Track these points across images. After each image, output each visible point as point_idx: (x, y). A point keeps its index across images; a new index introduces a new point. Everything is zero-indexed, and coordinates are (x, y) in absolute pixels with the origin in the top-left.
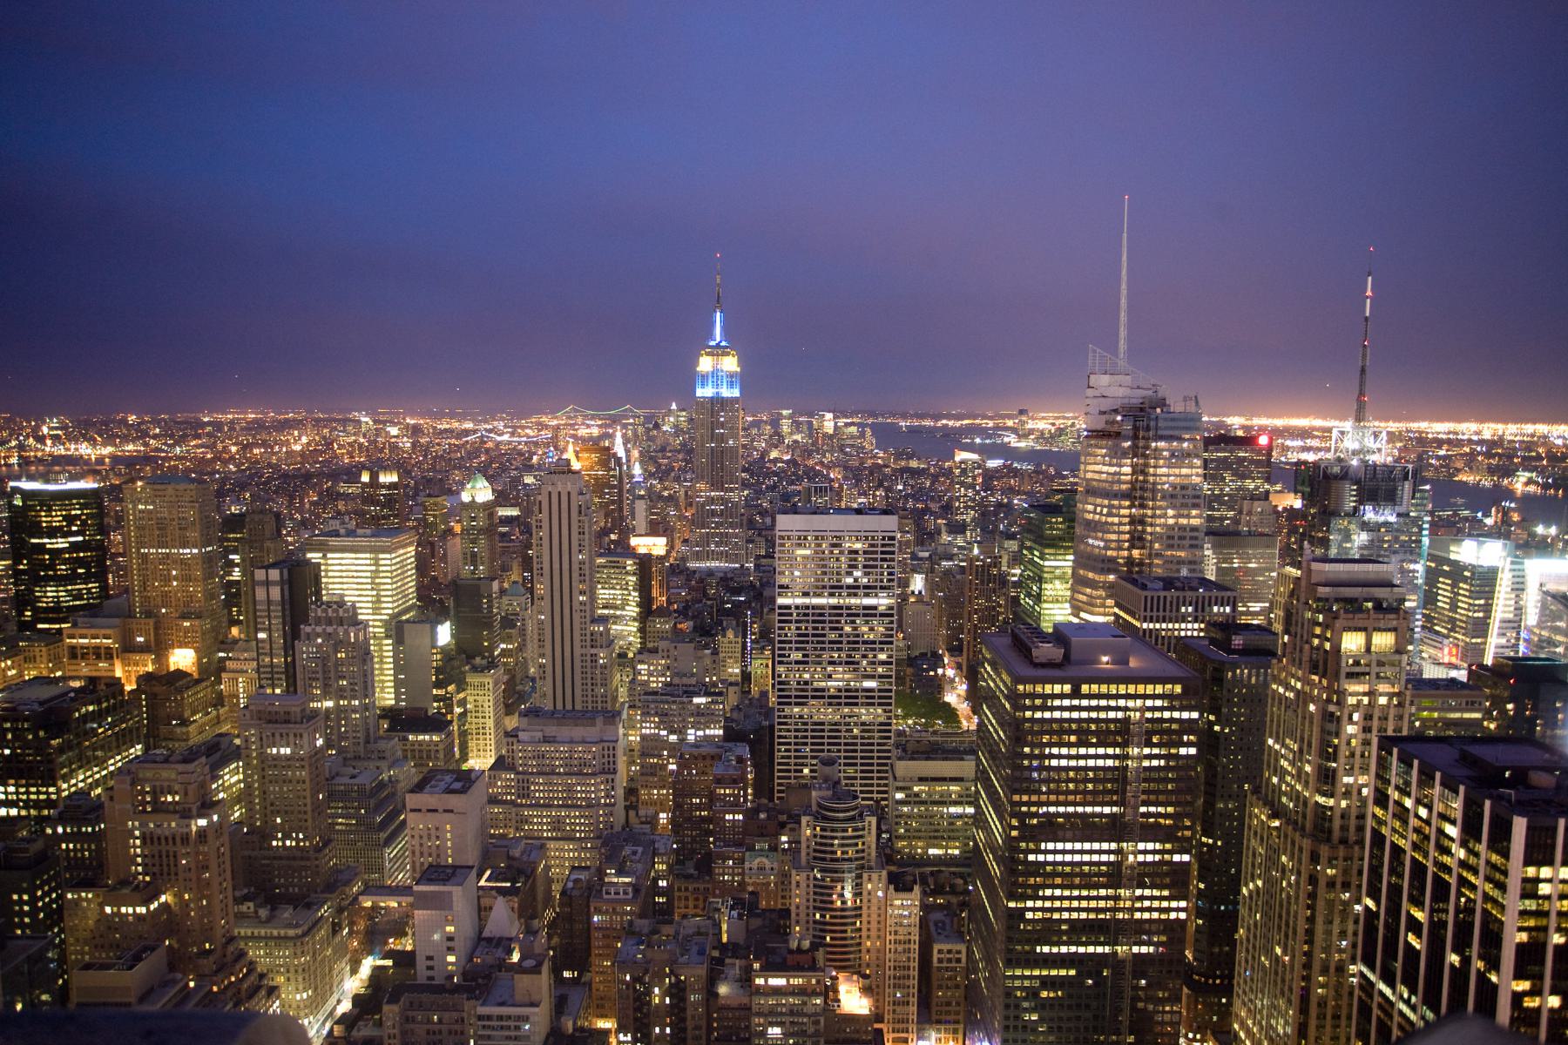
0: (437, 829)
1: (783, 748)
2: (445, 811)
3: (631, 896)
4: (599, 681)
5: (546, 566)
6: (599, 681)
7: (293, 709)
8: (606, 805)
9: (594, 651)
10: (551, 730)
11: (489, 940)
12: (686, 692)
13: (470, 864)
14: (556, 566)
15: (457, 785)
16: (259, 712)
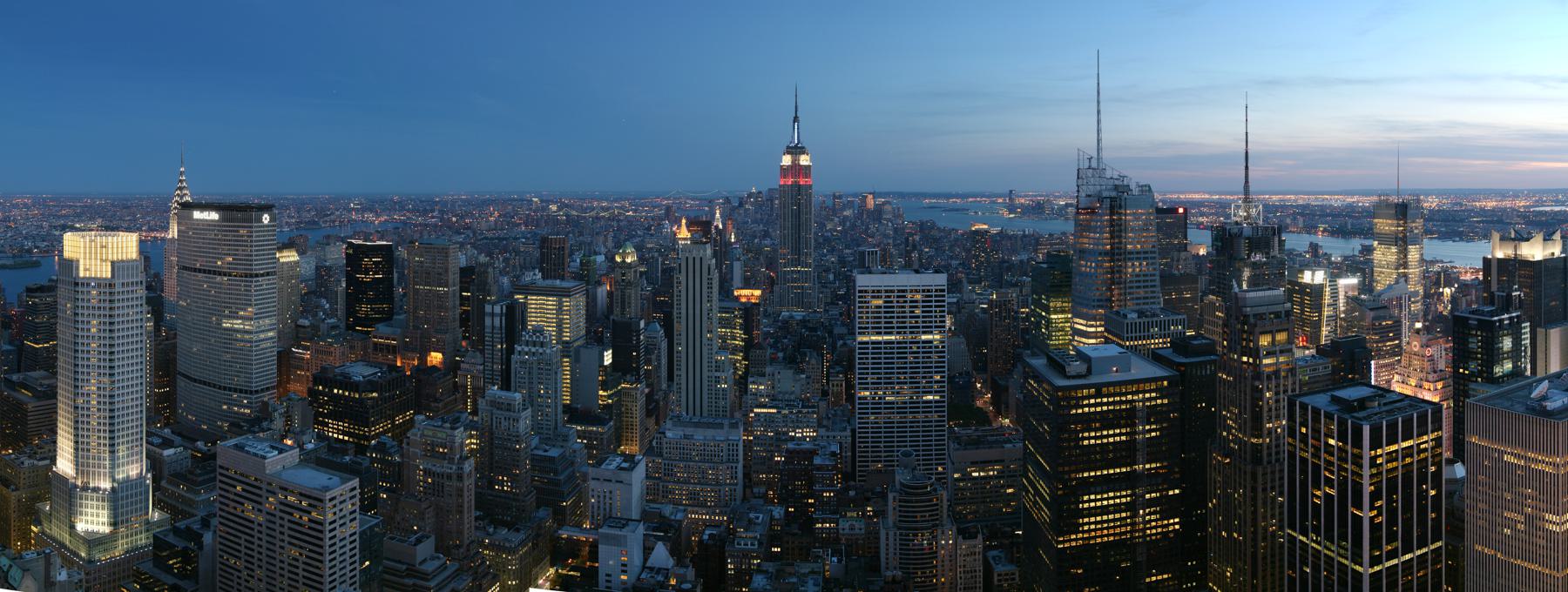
0: (611, 492)
1: (862, 445)
2: (617, 482)
3: (756, 547)
4: (721, 396)
5: (683, 311)
6: (721, 396)
7: (513, 402)
8: (730, 484)
9: (718, 374)
10: (689, 431)
11: (651, 569)
12: (787, 405)
13: (633, 518)
14: (691, 311)
15: (625, 465)
16: (491, 401)
